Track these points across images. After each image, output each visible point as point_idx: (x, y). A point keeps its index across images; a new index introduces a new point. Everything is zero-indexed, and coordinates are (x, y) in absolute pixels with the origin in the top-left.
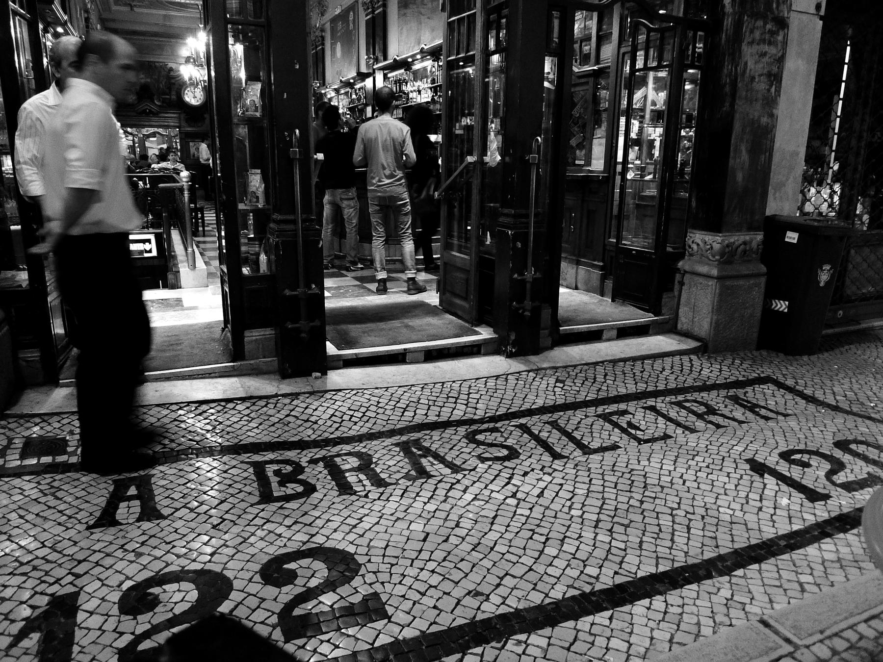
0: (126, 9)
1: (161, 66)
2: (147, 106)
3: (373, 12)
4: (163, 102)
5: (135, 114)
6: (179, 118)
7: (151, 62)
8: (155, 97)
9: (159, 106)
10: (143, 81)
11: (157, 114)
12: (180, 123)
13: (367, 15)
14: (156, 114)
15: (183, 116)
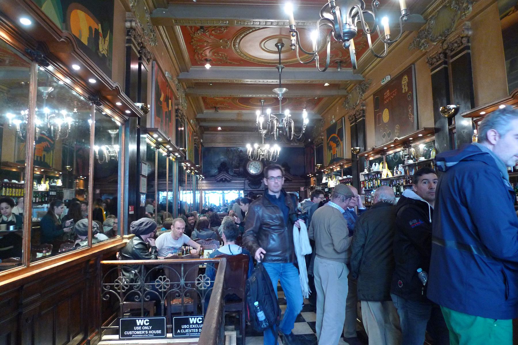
0: (212, 111)
1: (235, 150)
2: (223, 176)
3: (445, 63)
4: (234, 173)
5: (216, 182)
6: (244, 183)
7: (229, 147)
8: (229, 170)
9: (232, 176)
10: (222, 160)
11: (230, 181)
12: (244, 186)
13: (432, 70)
14: (229, 181)
15: (247, 181)
